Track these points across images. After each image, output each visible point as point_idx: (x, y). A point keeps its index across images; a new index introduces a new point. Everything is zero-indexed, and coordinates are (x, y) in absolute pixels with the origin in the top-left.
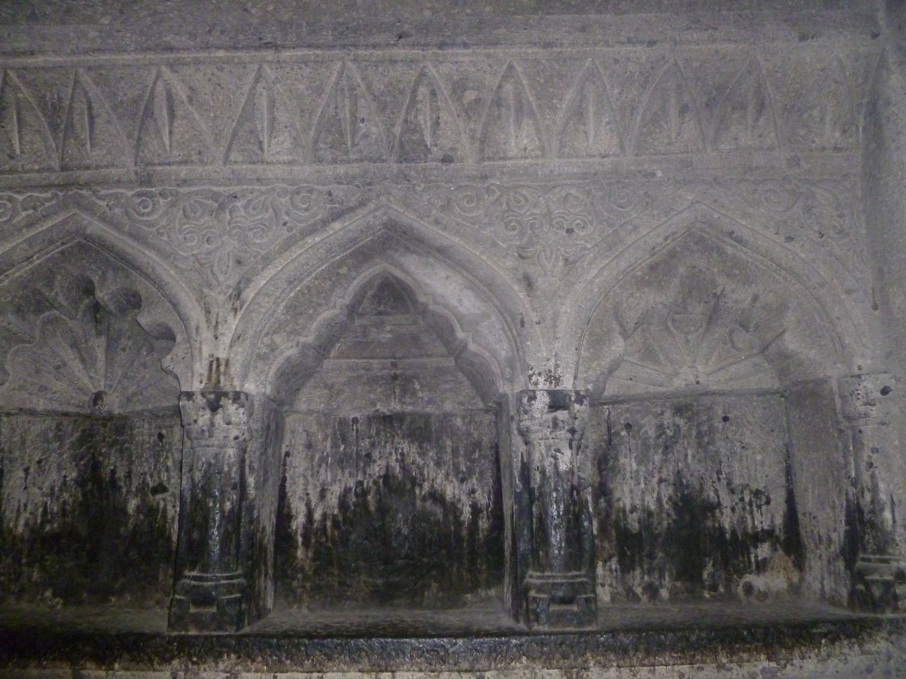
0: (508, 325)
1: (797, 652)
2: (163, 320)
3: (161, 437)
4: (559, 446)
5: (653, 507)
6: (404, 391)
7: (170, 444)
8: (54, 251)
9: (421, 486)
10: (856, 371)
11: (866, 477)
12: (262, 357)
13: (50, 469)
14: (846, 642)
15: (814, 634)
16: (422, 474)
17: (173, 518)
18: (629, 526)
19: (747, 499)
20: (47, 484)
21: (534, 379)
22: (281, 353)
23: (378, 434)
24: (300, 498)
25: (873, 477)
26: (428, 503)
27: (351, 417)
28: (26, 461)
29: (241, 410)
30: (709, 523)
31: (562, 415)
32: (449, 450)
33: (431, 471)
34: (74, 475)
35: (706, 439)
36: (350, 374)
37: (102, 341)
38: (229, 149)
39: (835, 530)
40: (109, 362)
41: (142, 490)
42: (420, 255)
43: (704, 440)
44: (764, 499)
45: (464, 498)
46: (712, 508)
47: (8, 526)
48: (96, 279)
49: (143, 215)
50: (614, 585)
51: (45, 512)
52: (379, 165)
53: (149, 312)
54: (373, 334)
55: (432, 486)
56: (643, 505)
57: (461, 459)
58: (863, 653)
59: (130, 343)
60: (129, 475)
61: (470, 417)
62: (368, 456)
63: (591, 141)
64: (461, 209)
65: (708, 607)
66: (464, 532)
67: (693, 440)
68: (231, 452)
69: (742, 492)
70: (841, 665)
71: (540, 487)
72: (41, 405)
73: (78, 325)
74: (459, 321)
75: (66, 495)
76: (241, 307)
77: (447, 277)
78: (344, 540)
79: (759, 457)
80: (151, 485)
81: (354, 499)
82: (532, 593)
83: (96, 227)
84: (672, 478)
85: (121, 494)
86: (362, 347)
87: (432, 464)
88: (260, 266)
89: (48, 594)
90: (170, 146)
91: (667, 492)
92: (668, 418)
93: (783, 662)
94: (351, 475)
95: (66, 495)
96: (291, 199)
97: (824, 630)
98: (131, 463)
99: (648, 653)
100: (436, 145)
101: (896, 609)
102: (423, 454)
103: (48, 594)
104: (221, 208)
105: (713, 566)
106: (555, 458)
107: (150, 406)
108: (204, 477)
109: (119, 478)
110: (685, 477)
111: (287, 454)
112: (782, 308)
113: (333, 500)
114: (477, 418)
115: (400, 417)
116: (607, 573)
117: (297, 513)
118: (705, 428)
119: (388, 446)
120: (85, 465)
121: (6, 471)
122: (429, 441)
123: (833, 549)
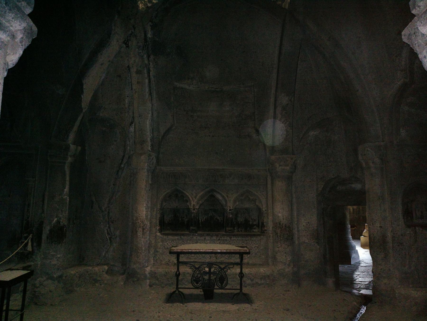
112: (256, 200)
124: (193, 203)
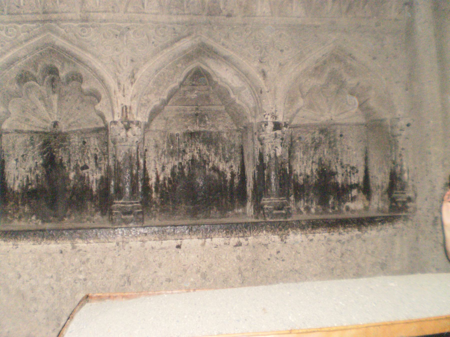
0: (254, 92)
2: (94, 87)
3: (84, 143)
4: (277, 145)
5: (309, 173)
6: (201, 120)
7: (89, 146)
8: (37, 53)
9: (208, 164)
10: (398, 116)
11: (398, 161)
12: (142, 105)
13: (28, 159)
16: (209, 159)
17: (93, 181)
19: (349, 170)
20: (28, 166)
21: (266, 116)
22: (152, 103)
23: (188, 141)
24: (153, 171)
25: (401, 160)
26: (212, 172)
27: (176, 133)
28: (16, 155)
29: (140, 129)
30: (332, 181)
31: (278, 132)
32: (221, 148)
33: (212, 157)
34: (41, 161)
35: (333, 144)
36: (176, 113)
37: (56, 97)
38: (127, 5)
39: (385, 182)
40: (60, 106)
41: (76, 168)
42: (214, 58)
43: (331, 145)
44: (356, 170)
45: (227, 169)
46: (333, 174)
47: (10, 187)
48: (59, 67)
49: (83, 36)
51: (28, 179)
52: (198, 16)
53: (87, 83)
54: (189, 95)
55: (213, 164)
56: (305, 173)
57: (226, 152)
58: (394, 228)
59: (70, 97)
60: (69, 161)
61: (230, 132)
62: (184, 151)
63: (294, 10)
64: (234, 38)
65: (331, 216)
66: (228, 185)
67: (327, 145)
68: (135, 148)
69: (346, 168)
70: (385, 233)
71: (268, 163)
72: (26, 128)
73: (44, 89)
74: (232, 90)
75: (38, 172)
76: (134, 82)
77: (227, 70)
78: (174, 189)
79: (354, 153)
80: (81, 166)
81: (178, 171)
82: (266, 206)
83: (59, 42)
84: (317, 161)
85: (65, 170)
86: (183, 101)
87: (213, 154)
88: (142, 63)
89: (34, 218)
90: (99, 4)
91: (315, 167)
92: (317, 135)
93: (364, 232)
94: (176, 160)
95: (38, 172)
96: (156, 31)
97: (380, 219)
98: (70, 155)
99: (313, 228)
100: (225, 9)
101: (406, 212)
102: (209, 150)
103: (34, 218)
104: (122, 34)
105: (334, 198)
106: (275, 150)
107: (81, 128)
108: (124, 159)
109: (64, 163)
111: (146, 150)
113: (168, 171)
114: (233, 134)
115: (199, 133)
117: (152, 177)
119: (193, 146)
120: (46, 157)
121: (6, 160)
122: (212, 144)
123: (384, 190)
124: (121, 101)
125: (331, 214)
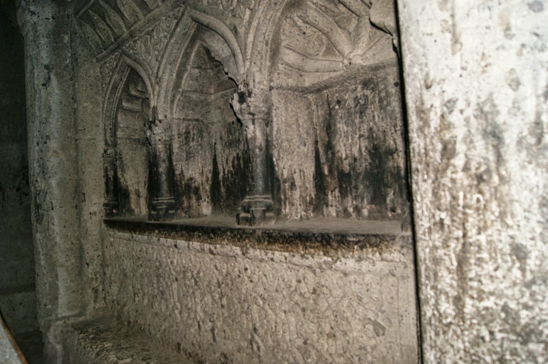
1: (340, 253)
5: (357, 155)
14: (370, 250)
15: (350, 241)
18: (344, 169)
30: (390, 164)
50: (338, 206)
56: (351, 154)
58: (382, 260)
62: (239, 140)
84: (366, 134)
91: (364, 143)
94: (235, 151)
99: (269, 243)
105: (394, 194)
110: (375, 133)
116: (334, 198)
118: (383, 94)
125: (390, 219)
